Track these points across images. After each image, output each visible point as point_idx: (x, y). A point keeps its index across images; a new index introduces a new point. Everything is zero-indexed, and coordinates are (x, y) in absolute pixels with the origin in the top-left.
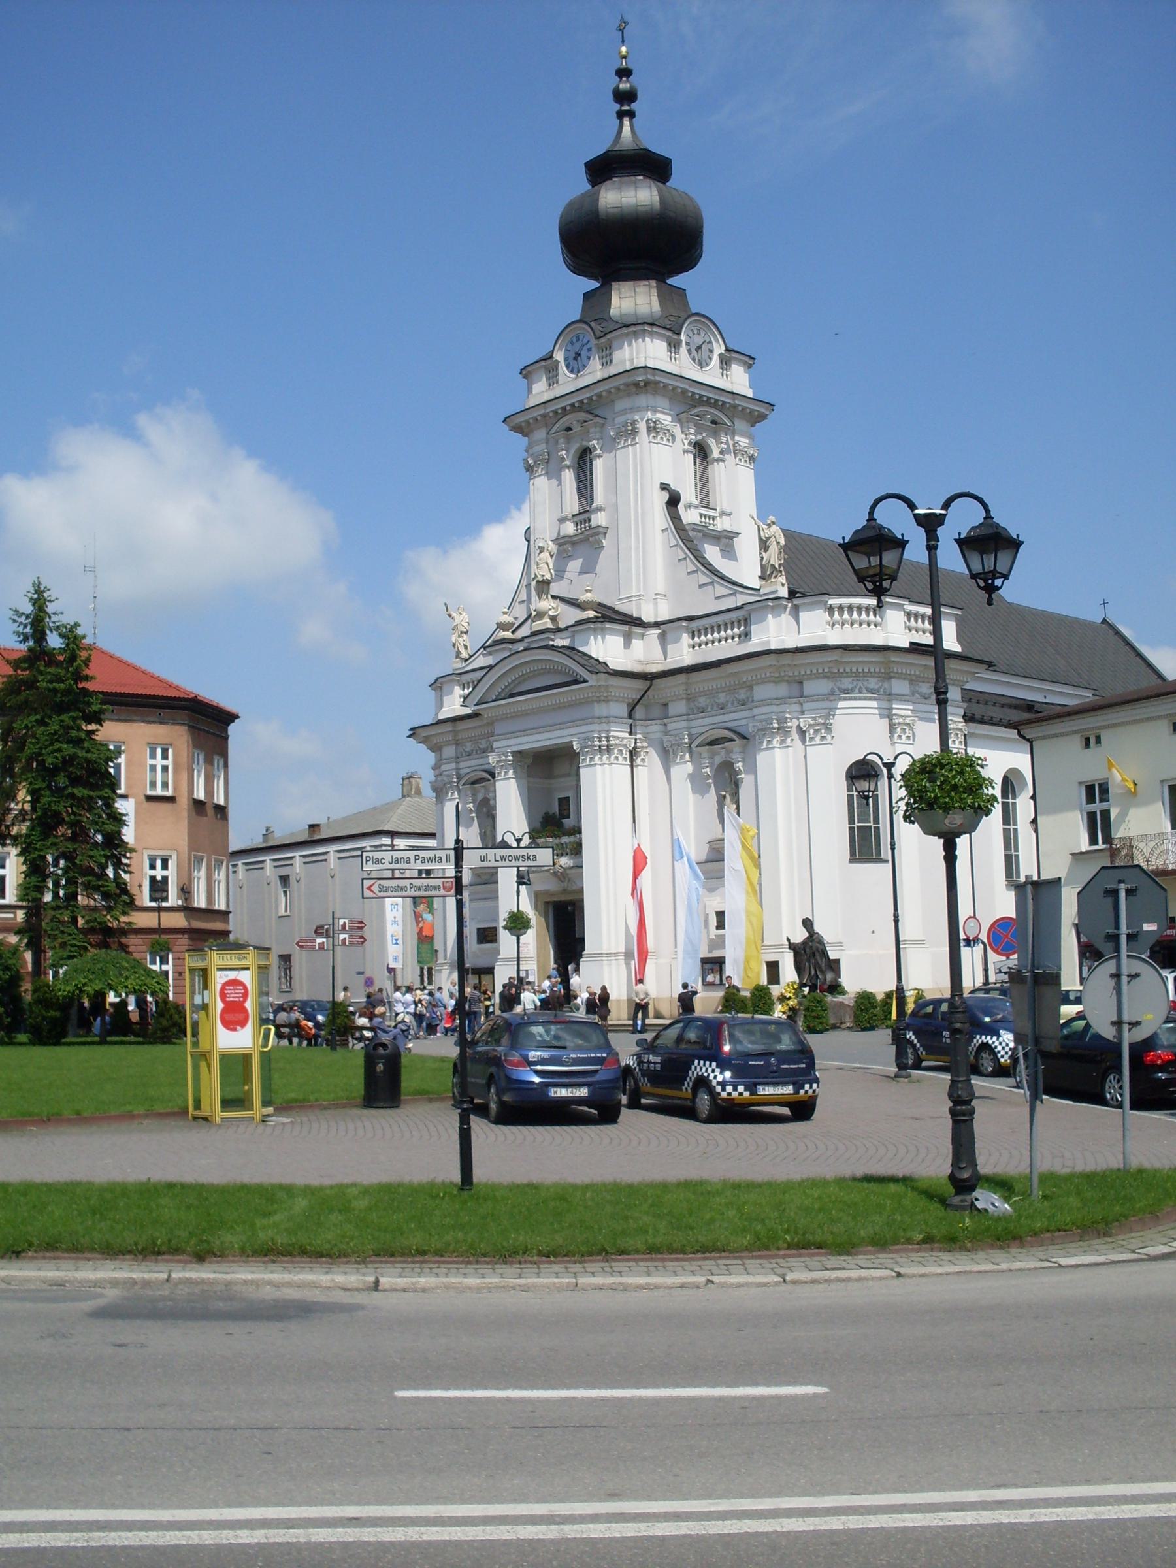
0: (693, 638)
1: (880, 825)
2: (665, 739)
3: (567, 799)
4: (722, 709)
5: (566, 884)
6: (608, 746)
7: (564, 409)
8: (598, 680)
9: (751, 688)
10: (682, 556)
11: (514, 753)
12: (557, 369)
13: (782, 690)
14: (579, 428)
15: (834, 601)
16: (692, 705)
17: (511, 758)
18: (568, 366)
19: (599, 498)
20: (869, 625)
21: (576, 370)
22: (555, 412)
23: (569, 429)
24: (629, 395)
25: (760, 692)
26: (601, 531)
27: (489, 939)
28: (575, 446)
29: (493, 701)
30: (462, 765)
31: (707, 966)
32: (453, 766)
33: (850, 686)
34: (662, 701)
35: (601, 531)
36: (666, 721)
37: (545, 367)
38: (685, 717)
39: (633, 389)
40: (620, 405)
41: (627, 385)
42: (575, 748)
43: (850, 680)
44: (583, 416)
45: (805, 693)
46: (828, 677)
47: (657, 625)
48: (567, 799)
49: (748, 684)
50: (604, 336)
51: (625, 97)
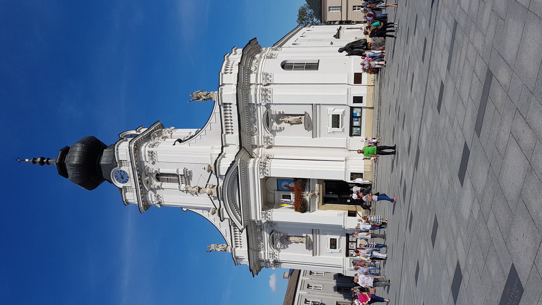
0: (229, 133)
1: (306, 63)
6: (264, 163)
7: (140, 184)
9: (249, 104)
11: (262, 210)
14: (148, 178)
15: (223, 71)
17: (264, 212)
18: (126, 182)
21: (127, 178)
23: (148, 182)
26: (185, 170)
27: (335, 243)
29: (241, 217)
31: (353, 134)
33: (254, 67)
35: (185, 170)
43: (252, 67)
44: (143, 174)
47: (222, 148)
49: (248, 105)
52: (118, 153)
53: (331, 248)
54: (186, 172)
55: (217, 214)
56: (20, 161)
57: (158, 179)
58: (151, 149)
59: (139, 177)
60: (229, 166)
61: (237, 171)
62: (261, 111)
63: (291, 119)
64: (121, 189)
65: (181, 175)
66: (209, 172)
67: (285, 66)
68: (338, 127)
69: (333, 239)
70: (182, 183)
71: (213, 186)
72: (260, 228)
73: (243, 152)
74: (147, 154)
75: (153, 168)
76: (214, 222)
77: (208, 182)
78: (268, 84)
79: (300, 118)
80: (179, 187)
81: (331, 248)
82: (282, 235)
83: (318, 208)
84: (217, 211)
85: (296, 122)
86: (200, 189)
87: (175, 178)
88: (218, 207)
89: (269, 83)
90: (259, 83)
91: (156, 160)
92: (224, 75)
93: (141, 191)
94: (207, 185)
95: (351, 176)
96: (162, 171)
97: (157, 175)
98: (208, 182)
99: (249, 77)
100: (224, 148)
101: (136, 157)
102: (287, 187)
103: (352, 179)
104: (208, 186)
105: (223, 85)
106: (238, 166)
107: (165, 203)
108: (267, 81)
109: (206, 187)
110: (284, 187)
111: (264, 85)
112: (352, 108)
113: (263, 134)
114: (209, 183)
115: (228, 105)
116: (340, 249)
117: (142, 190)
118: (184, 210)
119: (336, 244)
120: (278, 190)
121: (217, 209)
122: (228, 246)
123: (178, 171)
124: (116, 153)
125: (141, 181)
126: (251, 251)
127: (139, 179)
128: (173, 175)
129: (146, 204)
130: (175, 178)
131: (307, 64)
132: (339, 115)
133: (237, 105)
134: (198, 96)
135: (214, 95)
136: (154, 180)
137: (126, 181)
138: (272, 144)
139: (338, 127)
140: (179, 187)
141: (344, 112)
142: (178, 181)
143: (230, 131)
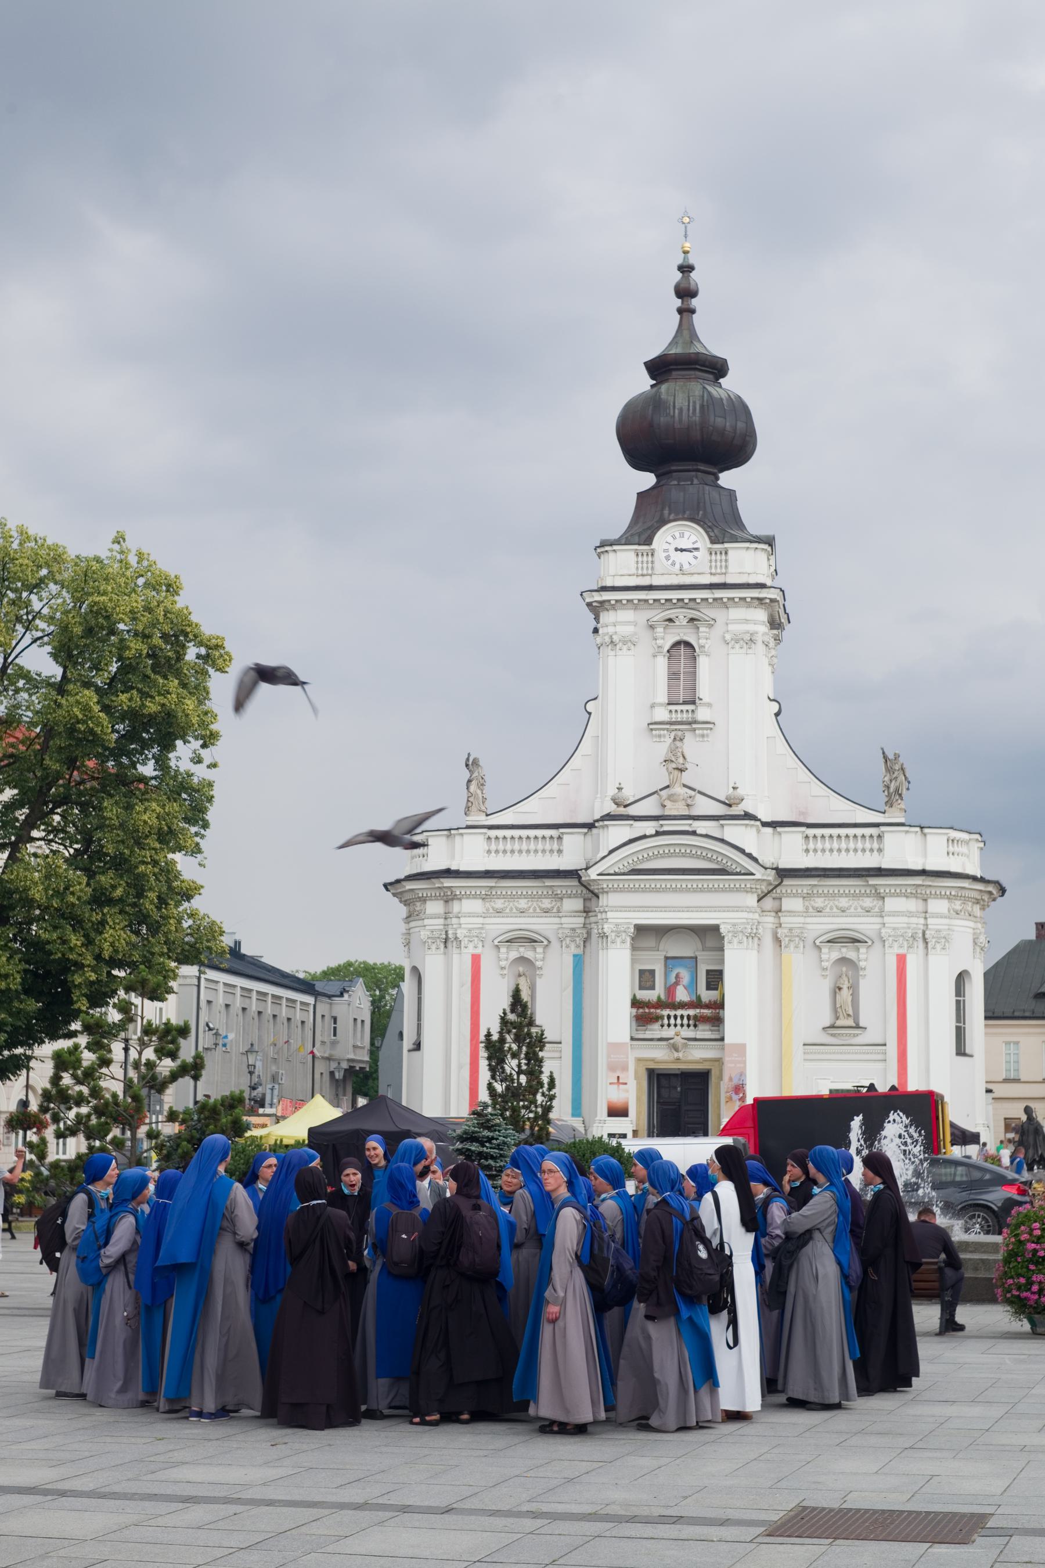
0: (807, 844)
2: (779, 930)
3: (652, 972)
4: (843, 911)
5: (680, 1055)
8: (763, 875)
9: (884, 898)
11: (636, 926)
12: (652, 555)
13: (912, 905)
14: (685, 623)
15: (954, 834)
16: (807, 903)
19: (704, 691)
20: (953, 854)
23: (670, 620)
25: (892, 904)
32: (480, 920)
34: (774, 895)
36: (780, 914)
38: (804, 914)
39: (757, 602)
40: (735, 613)
41: (752, 598)
42: (722, 931)
45: (929, 911)
46: (949, 898)
48: (652, 972)
49: (882, 895)
50: (723, 543)
54: (707, 729)
55: (610, 808)
56: (684, 223)
57: (677, 644)
58: (759, 638)
60: (747, 851)
62: (865, 925)
63: (845, 994)
64: (649, 541)
67: (961, 979)
70: (671, 711)
72: (553, 907)
73: (771, 875)
74: (751, 628)
77: (700, 792)
78: (925, 941)
79: (849, 1015)
80: (661, 705)
82: (539, 964)
83: (639, 1060)
84: (622, 811)
85: (838, 1006)
86: (681, 770)
87: (682, 691)
88: (632, 811)
89: (929, 945)
90: (930, 921)
91: (732, 651)
92: (945, 838)
93: (646, 601)
94: (694, 790)
96: (703, 662)
97: (688, 645)
98: (700, 792)
99: (942, 897)
101: (743, 599)
102: (674, 980)
104: (692, 793)
106: (753, 874)
107: (611, 660)
108: (934, 940)
109: (684, 786)
110: (673, 975)
114: (699, 796)
115: (876, 846)
118: (588, 705)
120: (667, 958)
121: (625, 806)
122: (487, 815)
123: (709, 705)
124: (747, 545)
126: (491, 883)
128: (694, 689)
129: (607, 605)
130: (682, 691)
131: (964, 1028)
133: (879, 872)
134: (896, 773)
136: (677, 638)
137: (670, 562)
138: (786, 947)
140: (661, 705)
142: (674, 700)
143: (811, 846)
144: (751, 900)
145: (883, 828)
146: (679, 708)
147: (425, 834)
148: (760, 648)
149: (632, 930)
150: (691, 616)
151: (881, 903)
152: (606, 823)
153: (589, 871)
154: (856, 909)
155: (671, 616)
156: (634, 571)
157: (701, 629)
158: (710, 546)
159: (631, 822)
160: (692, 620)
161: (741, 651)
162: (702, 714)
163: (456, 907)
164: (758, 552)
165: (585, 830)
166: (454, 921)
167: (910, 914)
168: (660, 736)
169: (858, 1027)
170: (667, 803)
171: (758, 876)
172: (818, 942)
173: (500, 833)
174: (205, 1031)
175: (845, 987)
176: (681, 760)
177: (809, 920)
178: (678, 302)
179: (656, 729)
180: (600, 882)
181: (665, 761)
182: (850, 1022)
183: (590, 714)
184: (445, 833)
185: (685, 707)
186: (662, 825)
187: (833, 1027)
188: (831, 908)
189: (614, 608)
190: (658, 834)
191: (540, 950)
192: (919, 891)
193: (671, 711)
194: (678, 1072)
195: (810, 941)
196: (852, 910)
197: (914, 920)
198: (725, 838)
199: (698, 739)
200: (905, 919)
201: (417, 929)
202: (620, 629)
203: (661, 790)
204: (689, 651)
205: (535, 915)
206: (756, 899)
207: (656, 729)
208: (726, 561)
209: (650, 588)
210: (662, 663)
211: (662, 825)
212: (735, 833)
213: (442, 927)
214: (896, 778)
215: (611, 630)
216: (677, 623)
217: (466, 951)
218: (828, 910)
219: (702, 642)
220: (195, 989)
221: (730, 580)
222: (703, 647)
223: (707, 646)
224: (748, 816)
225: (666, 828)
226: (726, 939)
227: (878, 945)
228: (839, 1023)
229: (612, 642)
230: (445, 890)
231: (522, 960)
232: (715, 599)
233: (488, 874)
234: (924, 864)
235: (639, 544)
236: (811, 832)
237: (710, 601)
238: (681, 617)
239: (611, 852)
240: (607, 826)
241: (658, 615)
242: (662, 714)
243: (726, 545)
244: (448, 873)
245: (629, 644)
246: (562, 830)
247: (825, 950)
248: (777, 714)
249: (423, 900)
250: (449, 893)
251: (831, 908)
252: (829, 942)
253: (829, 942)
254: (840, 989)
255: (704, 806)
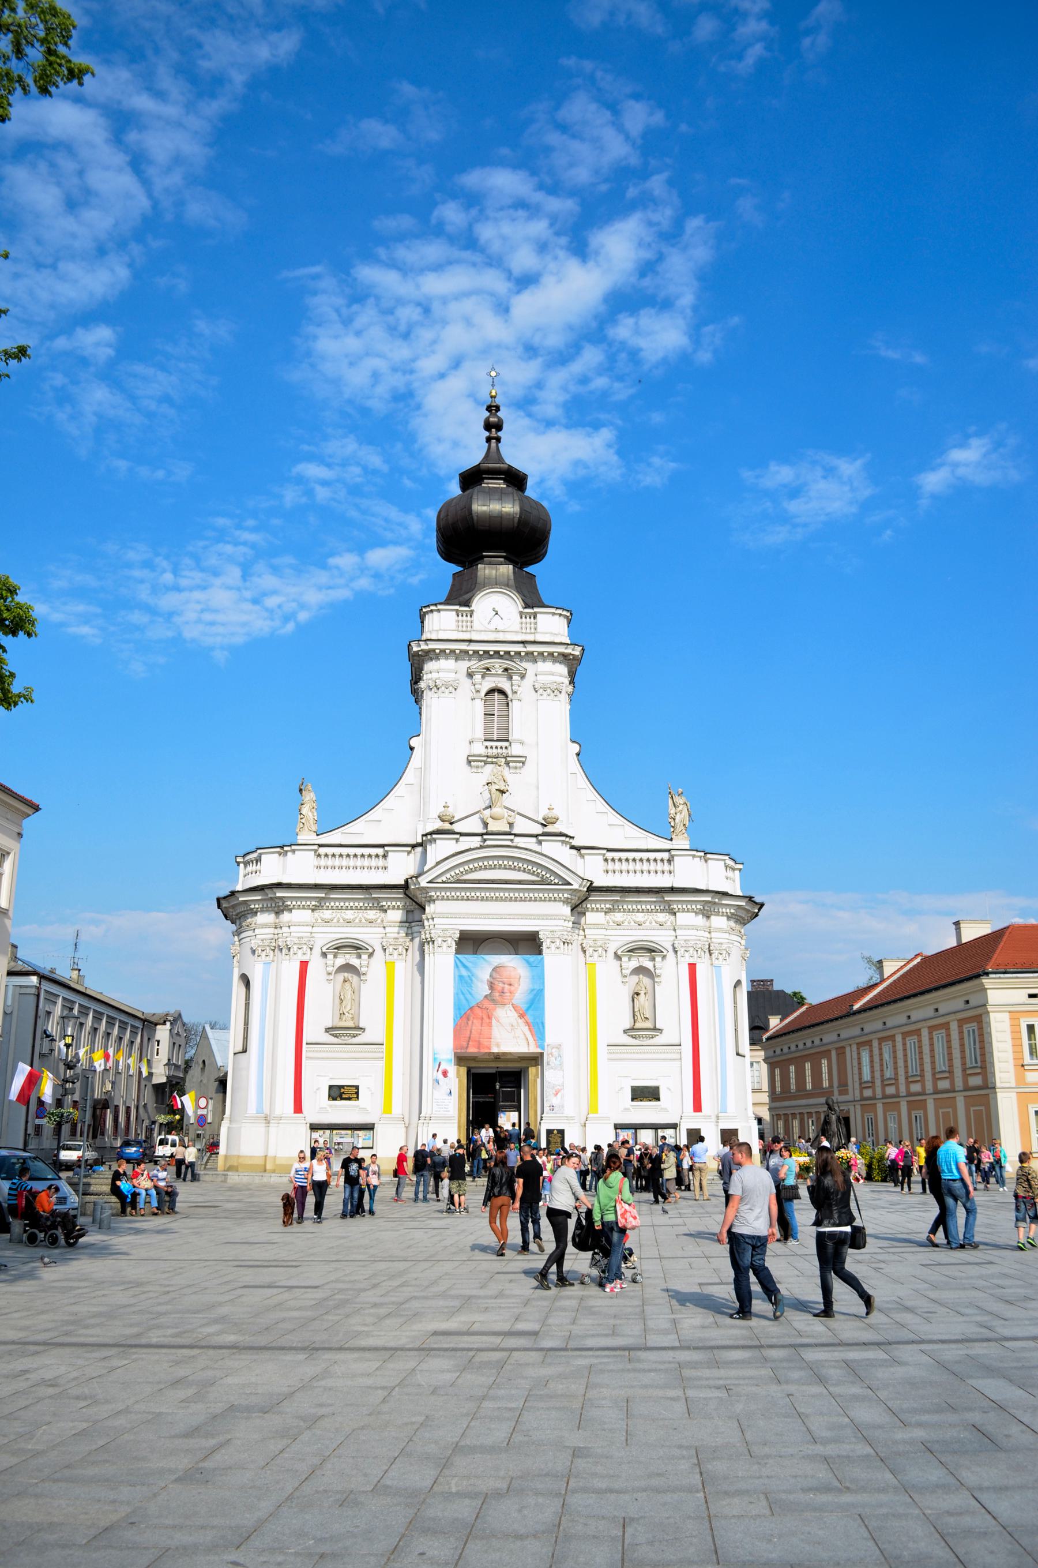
7: (486, 652)
9: (675, 914)
10: (594, 798)
13: (700, 920)
14: (500, 672)
22: (476, 652)
23: (488, 669)
24: (555, 661)
25: (682, 918)
27: (344, 1096)
28: (488, 684)
29: (443, 882)
30: (315, 930)
32: (309, 929)
37: (457, 611)
41: (560, 654)
51: (493, 427)
52: (554, 614)
53: (330, 1087)
54: (519, 762)
55: (438, 825)
57: (491, 691)
59: (502, 653)
61: (556, 881)
62: (662, 938)
64: (467, 603)
65: (506, 748)
66: (544, 819)
68: (633, 1100)
69: (357, 1093)
70: (487, 747)
71: (511, 825)
75: (522, 691)
76: (384, 807)
81: (330, 1087)
82: (363, 970)
84: (447, 826)
86: (502, 792)
87: (495, 731)
91: (541, 697)
93: (466, 652)
94: (514, 811)
95: (557, 1130)
97: (502, 692)
100: (574, 852)
101: (551, 654)
103: (549, 1132)
105: (706, 861)
111: (709, 945)
112: (674, 1126)
113: (611, 938)
115: (666, 867)
116: (328, 1108)
117: (471, 653)
119: (342, 1099)
121: (451, 824)
124: (553, 610)
125: (491, 657)
127: (497, 652)
129: (432, 655)
130: (495, 731)
132: (658, 1099)
133: (672, 890)
134: (681, 807)
135: (681, 842)
136: (492, 685)
139: (633, 1100)
141: (665, 1110)
144: (567, 910)
145: (673, 853)
146: (494, 744)
147: (259, 851)
148: (564, 698)
149: (458, 935)
150: (505, 666)
151: (672, 918)
152: (434, 836)
153: (419, 879)
154: (651, 923)
155: (488, 666)
156: (454, 628)
157: (514, 678)
158: (522, 610)
159: (457, 836)
160: (506, 670)
161: (548, 698)
162: (516, 750)
163: (286, 917)
164: (562, 618)
165: (409, 849)
166: (285, 929)
167: (696, 928)
168: (477, 767)
169: (655, 1029)
170: (490, 821)
171: (576, 886)
172: (619, 953)
173: (330, 851)
174: (42, 1038)
175: (642, 993)
176: (502, 783)
177: (609, 932)
178: (487, 434)
179: (474, 761)
180: (428, 890)
181: (488, 784)
182: (649, 1025)
183: (412, 749)
184: (278, 849)
185: (499, 744)
186: (485, 840)
187: (633, 1029)
188: (629, 923)
189: (437, 658)
190: (481, 847)
191: (365, 957)
192: (706, 908)
193: (487, 747)
194: (493, 1071)
195: (611, 954)
196: (647, 924)
197: (701, 933)
198: (544, 852)
199: (512, 771)
200: (694, 932)
201: (248, 939)
202: (441, 675)
203: (484, 809)
204: (502, 697)
205: (361, 925)
206: (569, 909)
207: (474, 761)
208: (535, 624)
209: (470, 641)
210: (479, 706)
211: (485, 840)
212: (553, 848)
213: (271, 936)
214: (680, 812)
215: (434, 675)
216: (493, 672)
217: (295, 956)
218: (626, 923)
219: (515, 688)
220: (33, 999)
221: (539, 638)
222: (516, 692)
223: (519, 693)
224: (561, 834)
225: (488, 843)
226: (544, 944)
227: (671, 955)
228: (638, 1025)
229: (436, 686)
230: (277, 901)
231: (348, 968)
232: (527, 653)
233: (317, 887)
234: (707, 884)
235: (460, 605)
236: (610, 855)
237: (523, 654)
238: (497, 666)
239: (438, 863)
240: (435, 840)
241: (474, 664)
242: (479, 749)
243: (536, 610)
244: (279, 885)
245: (451, 688)
246: (387, 848)
247: (625, 959)
248: (578, 755)
249: (255, 913)
250: (281, 904)
251: (629, 923)
252: (628, 951)
253: (628, 951)
254: (638, 994)
255: (522, 826)
